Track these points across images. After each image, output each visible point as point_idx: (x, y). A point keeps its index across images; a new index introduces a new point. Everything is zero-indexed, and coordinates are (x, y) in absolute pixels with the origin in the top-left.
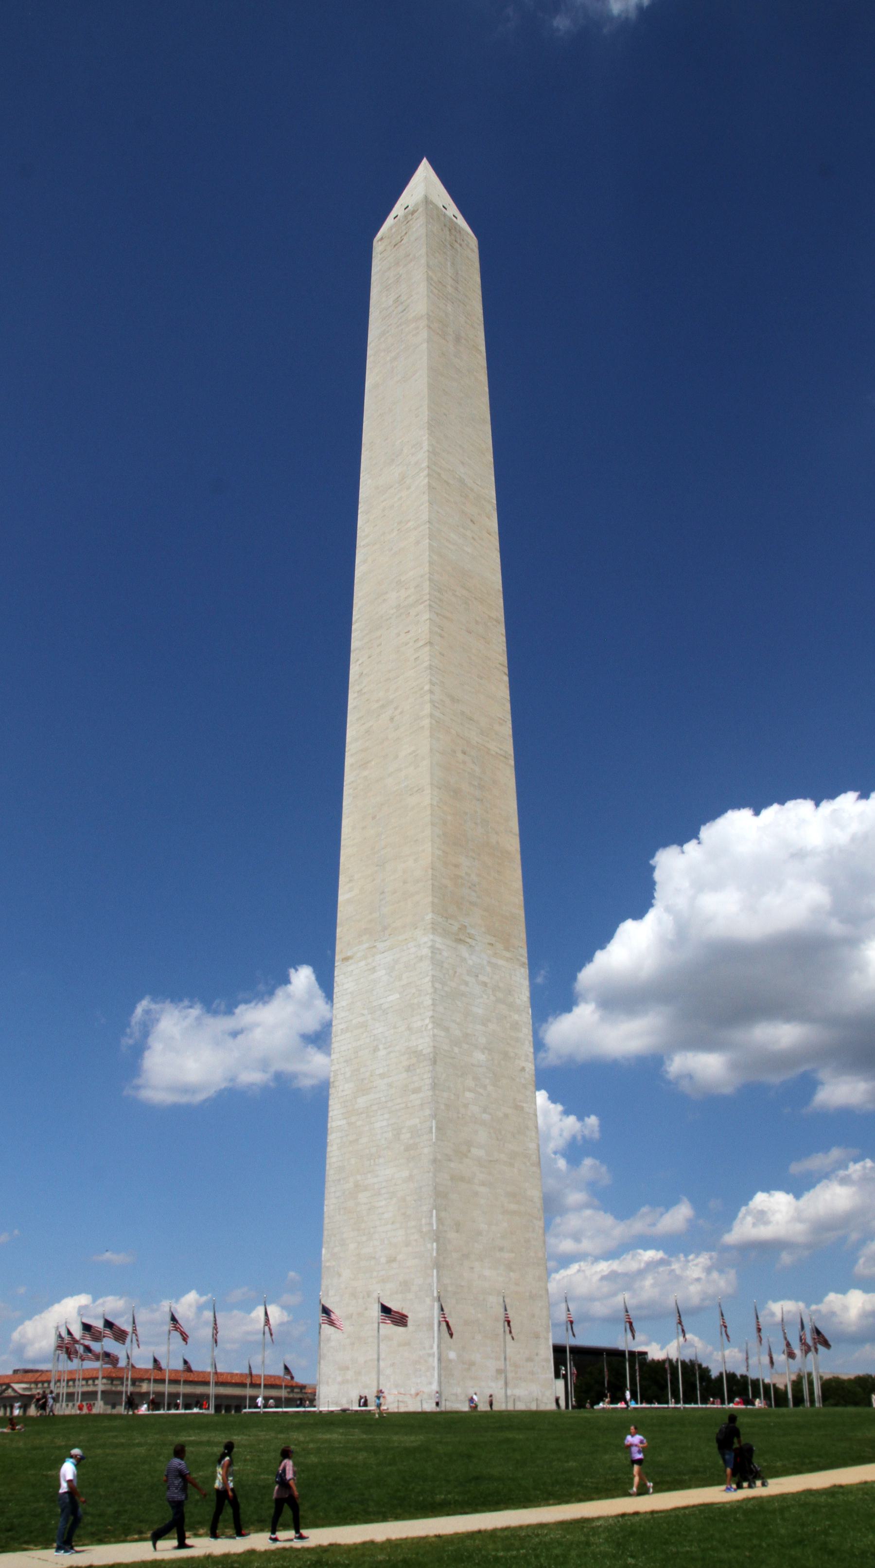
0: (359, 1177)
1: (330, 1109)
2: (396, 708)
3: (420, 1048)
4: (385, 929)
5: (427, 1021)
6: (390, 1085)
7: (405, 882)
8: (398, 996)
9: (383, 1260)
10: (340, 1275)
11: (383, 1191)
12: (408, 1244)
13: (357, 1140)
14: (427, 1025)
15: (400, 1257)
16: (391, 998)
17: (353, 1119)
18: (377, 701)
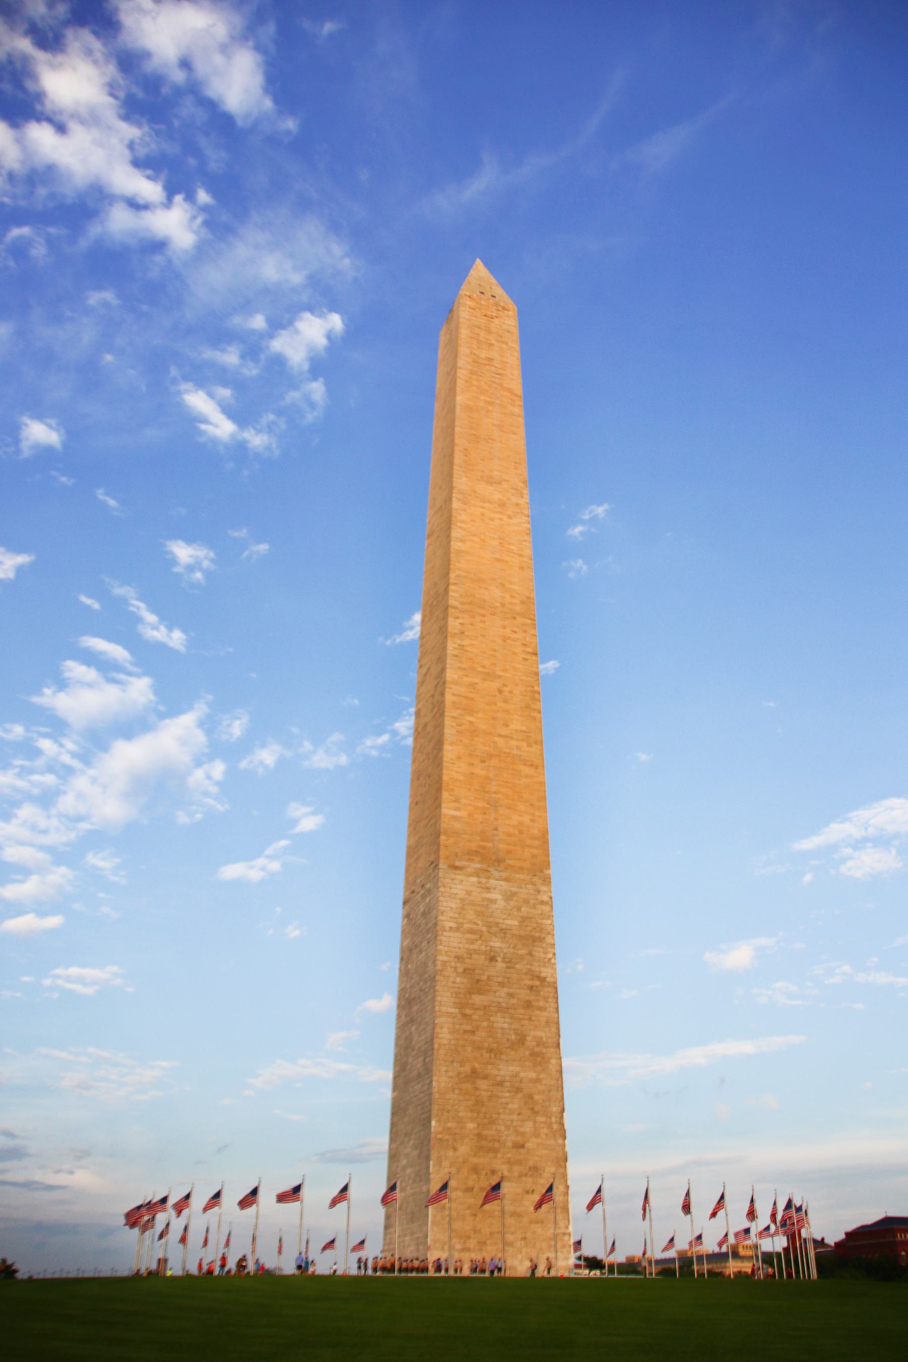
0: (477, 1065)
1: (437, 993)
2: (505, 685)
3: (543, 975)
4: (499, 861)
6: (511, 995)
7: (521, 832)
8: (516, 923)
9: (509, 1144)
10: (455, 1149)
12: (537, 1136)
14: (550, 959)
15: (528, 1145)
16: (509, 922)
17: (468, 1011)
18: (483, 667)
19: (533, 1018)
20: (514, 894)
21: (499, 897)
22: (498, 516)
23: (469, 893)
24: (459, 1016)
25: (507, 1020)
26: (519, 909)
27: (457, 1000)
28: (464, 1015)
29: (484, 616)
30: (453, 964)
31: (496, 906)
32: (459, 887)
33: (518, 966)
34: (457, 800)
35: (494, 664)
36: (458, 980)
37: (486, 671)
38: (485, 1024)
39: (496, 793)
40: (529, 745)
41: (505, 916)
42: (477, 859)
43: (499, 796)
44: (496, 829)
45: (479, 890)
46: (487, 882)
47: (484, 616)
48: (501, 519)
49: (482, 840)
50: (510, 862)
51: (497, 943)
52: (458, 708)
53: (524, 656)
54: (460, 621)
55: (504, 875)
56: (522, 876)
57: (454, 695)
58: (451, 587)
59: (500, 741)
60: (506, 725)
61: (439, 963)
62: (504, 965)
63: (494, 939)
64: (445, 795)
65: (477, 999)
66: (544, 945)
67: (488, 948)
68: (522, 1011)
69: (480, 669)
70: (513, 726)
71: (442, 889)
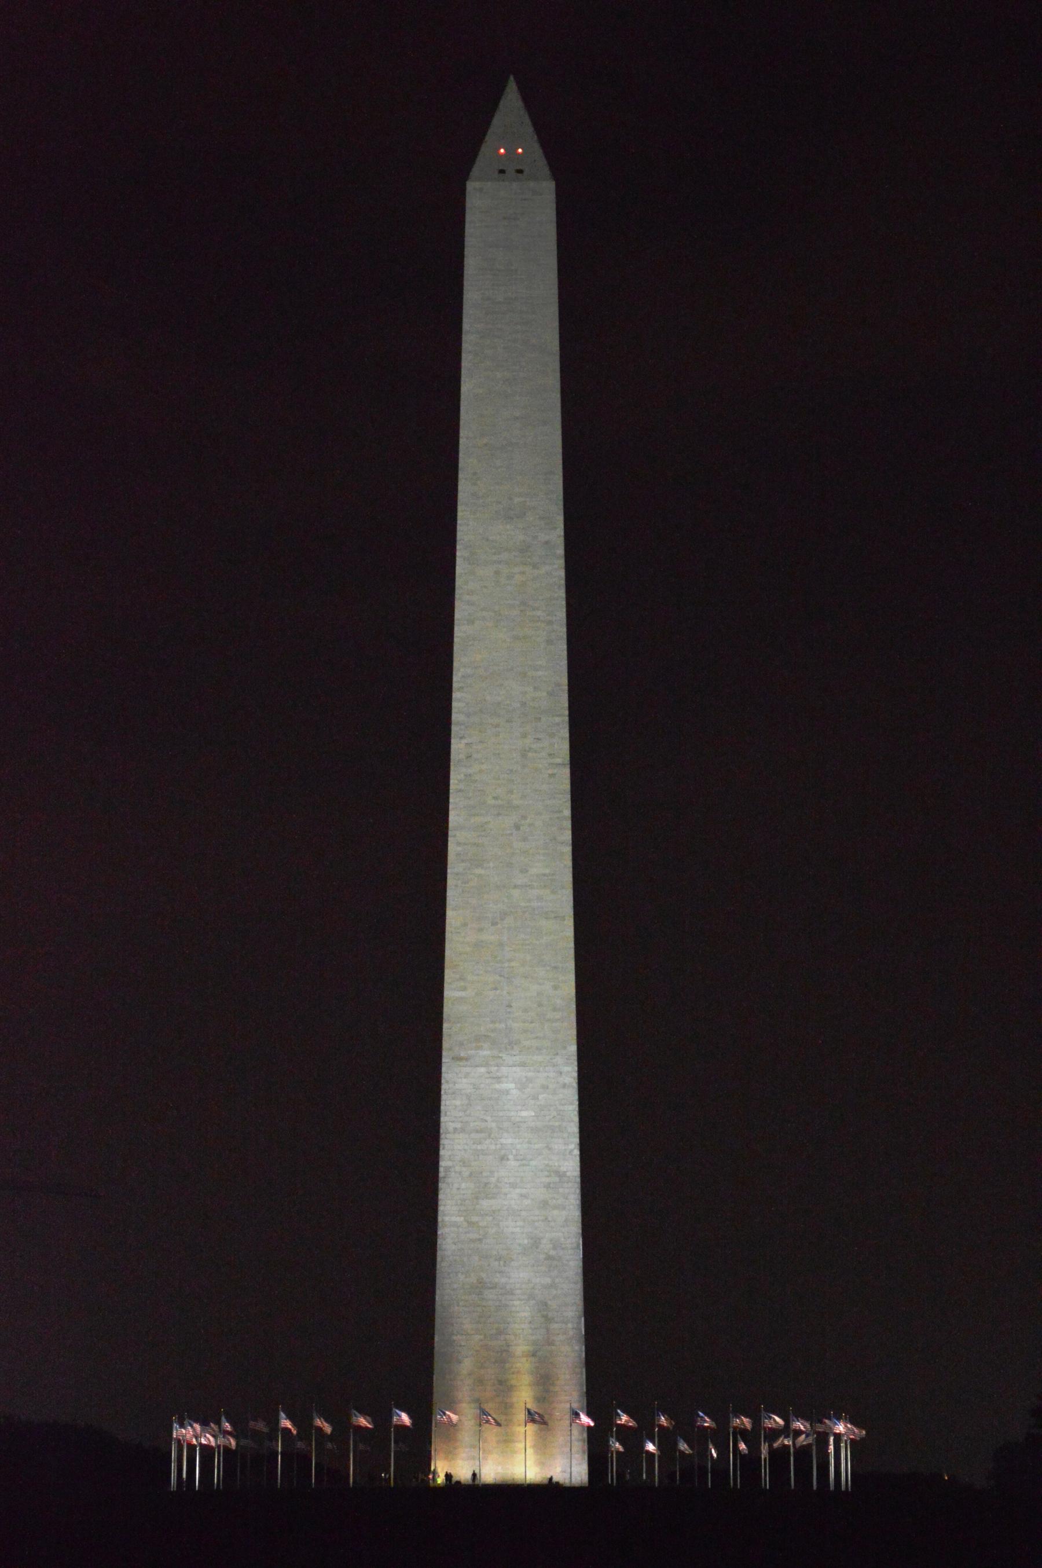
0: (483, 1275)
1: (440, 1203)
4: (511, 1044)
5: (572, 1146)
6: (523, 1196)
7: (540, 1005)
11: (518, 1292)
13: (480, 1240)
16: (524, 1114)
17: (475, 1219)
18: (495, 798)
19: (550, 1219)
20: (529, 1080)
21: (512, 1086)
22: (516, 570)
23: (476, 1087)
24: (465, 1224)
25: (518, 1224)
26: (535, 1098)
27: (463, 1208)
28: (470, 1224)
29: (497, 726)
30: (457, 1168)
31: (509, 1097)
32: (464, 1080)
33: (533, 1163)
34: (462, 979)
35: (511, 792)
36: (463, 1185)
37: (500, 802)
38: (494, 1230)
39: (510, 960)
40: (553, 892)
41: (519, 1108)
42: (486, 1045)
43: (513, 964)
44: (510, 1006)
45: (488, 1081)
46: (497, 1071)
47: (497, 726)
48: (523, 573)
49: (493, 1022)
50: (527, 1043)
51: (507, 1140)
52: (463, 861)
53: (550, 772)
54: (464, 741)
55: (517, 1058)
56: (540, 1058)
57: (459, 844)
58: (454, 695)
59: (516, 893)
60: (524, 871)
61: (441, 1169)
62: (517, 1164)
63: (505, 1135)
65: (485, 1204)
66: (565, 1135)
67: (498, 1146)
68: (537, 1212)
69: (493, 802)
70: (534, 871)
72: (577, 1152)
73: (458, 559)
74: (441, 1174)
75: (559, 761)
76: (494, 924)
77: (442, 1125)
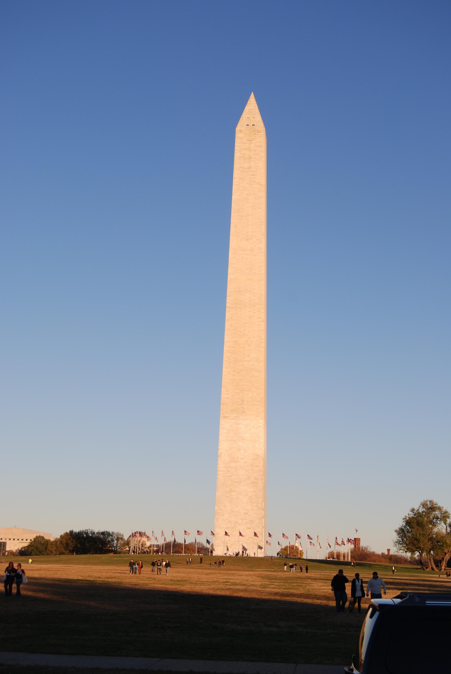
4: (243, 412)
6: (246, 462)
10: (223, 515)
17: (229, 469)
29: (241, 308)
47: (241, 308)
58: (227, 298)
60: (249, 356)
61: (219, 453)
64: (223, 389)
71: (220, 426)
72: (263, 448)
73: (230, 253)
74: (219, 455)
75: (261, 320)
76: (238, 373)
77: (220, 439)
